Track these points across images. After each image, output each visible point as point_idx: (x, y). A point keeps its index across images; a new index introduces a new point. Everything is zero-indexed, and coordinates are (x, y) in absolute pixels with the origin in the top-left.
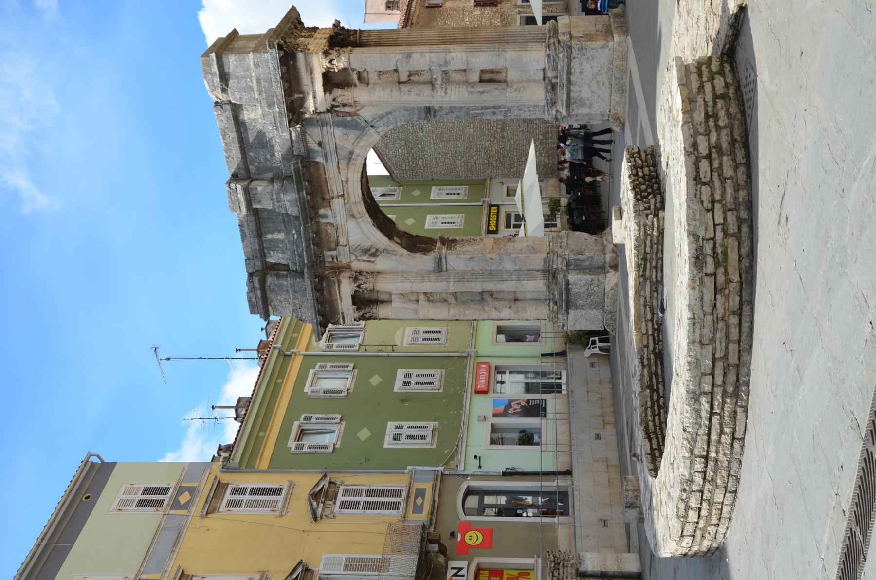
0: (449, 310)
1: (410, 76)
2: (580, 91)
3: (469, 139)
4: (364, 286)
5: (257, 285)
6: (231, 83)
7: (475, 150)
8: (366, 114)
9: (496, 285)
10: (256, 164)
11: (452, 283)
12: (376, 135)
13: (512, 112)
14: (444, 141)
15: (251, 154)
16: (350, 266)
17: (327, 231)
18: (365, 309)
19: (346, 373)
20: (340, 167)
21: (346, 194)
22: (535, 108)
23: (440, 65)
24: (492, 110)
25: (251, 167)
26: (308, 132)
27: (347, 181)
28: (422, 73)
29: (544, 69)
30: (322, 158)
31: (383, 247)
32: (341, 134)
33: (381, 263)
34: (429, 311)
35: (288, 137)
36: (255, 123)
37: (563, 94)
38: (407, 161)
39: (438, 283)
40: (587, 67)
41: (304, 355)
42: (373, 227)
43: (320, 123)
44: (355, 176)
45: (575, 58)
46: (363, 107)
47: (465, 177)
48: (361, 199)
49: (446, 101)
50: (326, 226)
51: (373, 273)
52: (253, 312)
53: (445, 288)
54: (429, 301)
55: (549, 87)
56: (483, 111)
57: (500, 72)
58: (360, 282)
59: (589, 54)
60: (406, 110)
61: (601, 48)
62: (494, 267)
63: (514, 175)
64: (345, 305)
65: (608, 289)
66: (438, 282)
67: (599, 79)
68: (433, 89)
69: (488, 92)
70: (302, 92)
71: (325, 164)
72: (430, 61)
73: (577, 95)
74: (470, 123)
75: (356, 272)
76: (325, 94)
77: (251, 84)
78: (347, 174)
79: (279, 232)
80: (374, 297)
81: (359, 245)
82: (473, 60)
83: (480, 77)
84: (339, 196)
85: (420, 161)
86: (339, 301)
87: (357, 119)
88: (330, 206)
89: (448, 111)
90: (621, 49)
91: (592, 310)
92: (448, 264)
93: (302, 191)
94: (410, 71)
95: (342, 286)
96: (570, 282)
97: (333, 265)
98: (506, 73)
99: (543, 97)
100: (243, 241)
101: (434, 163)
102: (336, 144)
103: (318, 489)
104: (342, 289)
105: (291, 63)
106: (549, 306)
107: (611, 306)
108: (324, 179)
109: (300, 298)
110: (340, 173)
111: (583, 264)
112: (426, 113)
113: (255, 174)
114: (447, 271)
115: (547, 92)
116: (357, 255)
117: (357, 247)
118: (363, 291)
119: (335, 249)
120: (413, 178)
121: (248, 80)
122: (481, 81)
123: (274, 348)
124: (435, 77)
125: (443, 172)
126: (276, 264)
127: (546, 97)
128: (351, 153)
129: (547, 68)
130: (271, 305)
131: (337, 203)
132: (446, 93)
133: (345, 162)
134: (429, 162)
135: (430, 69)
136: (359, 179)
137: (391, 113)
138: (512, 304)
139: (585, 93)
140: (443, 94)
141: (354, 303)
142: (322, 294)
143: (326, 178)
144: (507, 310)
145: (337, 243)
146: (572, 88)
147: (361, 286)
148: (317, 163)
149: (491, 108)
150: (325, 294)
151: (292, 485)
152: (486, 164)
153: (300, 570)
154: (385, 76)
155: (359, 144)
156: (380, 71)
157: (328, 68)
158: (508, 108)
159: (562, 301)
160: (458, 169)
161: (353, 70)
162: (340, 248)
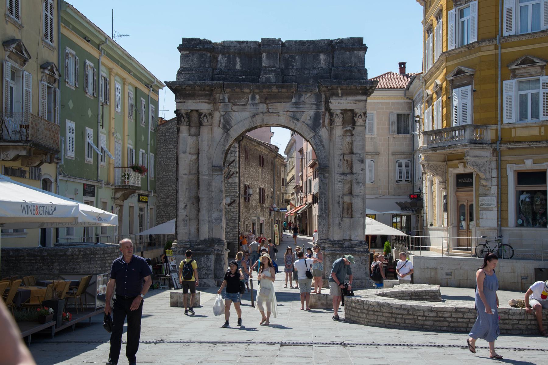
0: (186, 174)
1: (347, 161)
6: (348, 53)
8: (324, 132)
9: (206, 206)
10: (290, 59)
11: (207, 178)
15: (297, 57)
17: (243, 98)
18: (187, 118)
19: (92, 91)
20: (288, 112)
23: (356, 179)
25: (288, 55)
26: (312, 95)
29: (350, 240)
31: (230, 134)
32: (310, 115)
33: (218, 132)
34: (185, 161)
36: (318, 63)
38: (172, 137)
41: (99, 60)
43: (319, 103)
45: (360, 258)
46: (330, 131)
47: (158, 178)
52: (184, 40)
53: (204, 172)
55: (341, 242)
58: (208, 117)
61: (366, 273)
62: (214, 206)
63: (158, 213)
64: (191, 105)
69: (339, 207)
70: (342, 95)
71: (291, 103)
77: (347, 66)
79: (241, 67)
80: (192, 124)
81: (232, 118)
82: (359, 199)
85: (173, 147)
86: (194, 101)
88: (261, 103)
93: (276, 87)
94: (352, 161)
95: (206, 104)
97: (217, 99)
100: (236, 41)
101: (171, 156)
103: (55, 71)
104: (204, 104)
105: (361, 92)
106: (188, 242)
110: (285, 111)
113: (284, 57)
114: (213, 174)
116: (224, 117)
117: (230, 117)
119: (229, 102)
120: (158, 140)
121: (350, 64)
122: (343, 202)
123: (106, 39)
124: (348, 175)
125: (162, 162)
126: (217, 61)
127: (336, 241)
128: (298, 120)
129: (352, 242)
130: (188, 54)
131: (262, 107)
132: (339, 182)
134: (171, 152)
137: (323, 147)
140: (339, 180)
141: (192, 111)
143: (281, 102)
144: (185, 213)
145: (234, 104)
150: (200, 92)
151: (54, 48)
153: (26, 56)
156: (352, 143)
157: (356, 114)
160: (165, 173)
161: (354, 128)
162: (231, 105)
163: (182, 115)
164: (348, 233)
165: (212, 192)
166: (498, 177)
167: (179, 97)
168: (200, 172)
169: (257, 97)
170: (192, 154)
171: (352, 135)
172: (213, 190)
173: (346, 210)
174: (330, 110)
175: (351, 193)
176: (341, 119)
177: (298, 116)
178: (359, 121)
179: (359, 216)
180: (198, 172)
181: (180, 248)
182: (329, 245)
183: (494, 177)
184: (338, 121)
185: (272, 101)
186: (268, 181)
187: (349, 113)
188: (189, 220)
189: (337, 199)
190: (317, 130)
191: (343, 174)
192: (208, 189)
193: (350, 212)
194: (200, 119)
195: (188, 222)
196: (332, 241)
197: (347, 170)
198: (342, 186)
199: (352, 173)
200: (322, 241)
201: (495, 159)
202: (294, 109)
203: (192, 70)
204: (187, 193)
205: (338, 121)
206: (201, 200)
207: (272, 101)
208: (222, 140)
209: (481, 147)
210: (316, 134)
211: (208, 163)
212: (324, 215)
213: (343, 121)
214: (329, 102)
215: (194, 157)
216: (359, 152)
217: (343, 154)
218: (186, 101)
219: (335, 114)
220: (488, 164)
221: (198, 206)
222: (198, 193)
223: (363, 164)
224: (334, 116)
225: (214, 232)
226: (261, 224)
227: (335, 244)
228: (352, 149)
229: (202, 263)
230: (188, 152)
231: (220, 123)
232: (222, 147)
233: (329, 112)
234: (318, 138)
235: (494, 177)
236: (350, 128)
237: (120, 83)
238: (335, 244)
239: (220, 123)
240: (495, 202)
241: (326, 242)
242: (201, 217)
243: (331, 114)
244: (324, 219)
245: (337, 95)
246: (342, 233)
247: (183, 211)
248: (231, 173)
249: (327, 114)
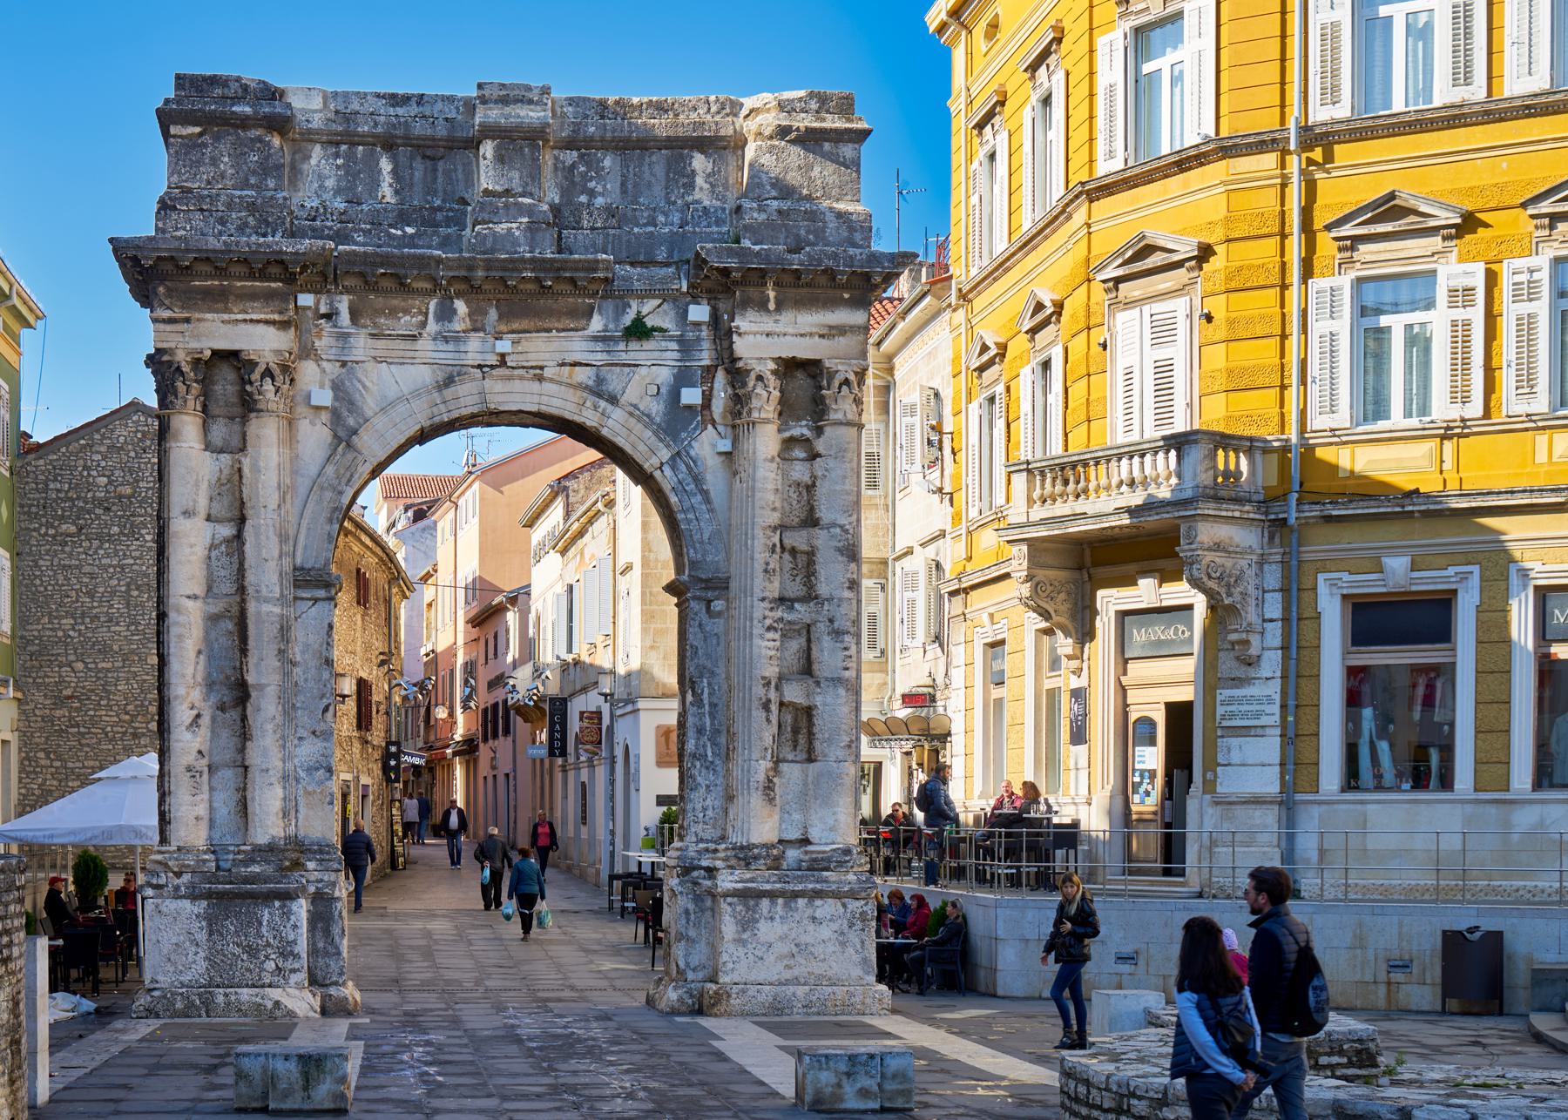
0: (195, 597)
2: (772, 919)
3: (132, 652)
4: (268, 386)
7: (100, 666)
12: (655, 461)
13: (704, 771)
16: (307, 357)
17: (406, 311)
21: (507, 372)
23: (831, 621)
27: (540, 379)
28: (798, 579)
29: (805, 841)
30: (600, 328)
35: (659, 259)
37: (768, 882)
39: (275, 578)
40: (826, 932)
42: (418, 427)
44: (556, 402)
45: (844, 906)
48: (492, 406)
49: (751, 627)
50: (420, 312)
53: (264, 591)
54: (210, 550)
55: (775, 852)
56: (707, 707)
59: (853, 937)
65: (275, 994)
66: (281, 574)
67: (798, 958)
68: (774, 601)
69: (768, 720)
72: (840, 600)
73: (765, 911)
76: (773, 359)
78: (559, 383)
80: (214, 409)
81: (364, 387)
83: (791, 703)
89: (708, 629)
90: (868, 1001)
91: (206, 958)
92: (311, 603)
94: (811, 554)
96: (288, 903)
98: (792, 761)
99: (755, 840)
102: (637, 366)
107: (228, 1004)
108: (545, 326)
110: (563, 364)
111: (319, 934)
112: (707, 581)
114: (296, 598)
115: (768, 846)
118: (251, 383)
122: (782, 704)
124: (797, 605)
127: (757, 847)
128: (613, 400)
129: (810, 848)
132: (769, 629)
133: (591, 383)
135: (816, 597)
136: (544, 409)
137: (707, 500)
138: (205, 762)
139: (767, 930)
140: (768, 622)
143: (548, 330)
146: (780, 901)
147: (269, 380)
148: (590, 316)
149: (712, 724)
152: (61, 691)
154: (795, 496)
155: (633, 421)
156: (810, 488)
158: (712, 763)
159: (231, 883)
161: (819, 431)
163: (178, 369)
164: (796, 816)
165: (294, 664)
166: (1286, 620)
168: (250, 590)
169: (461, 306)
170: (218, 521)
171: (814, 456)
172: (298, 658)
174: (734, 360)
175: (807, 669)
176: (776, 394)
177: (614, 385)
178: (842, 408)
179: (841, 754)
180: (242, 590)
181: (178, 875)
182: (733, 862)
183: (1271, 620)
184: (765, 403)
185: (515, 326)
187: (800, 375)
188: (210, 767)
189: (759, 690)
190: (684, 435)
191: (782, 600)
192: (280, 652)
193: (802, 740)
194: (248, 388)
195: (206, 776)
196: (742, 848)
197: (795, 589)
198: (778, 643)
199: (810, 597)
200: (702, 846)
201: (1276, 553)
202: (599, 356)
204: (201, 667)
205: (765, 403)
206: (253, 694)
207: (515, 326)
208: (330, 470)
209: (1237, 514)
210: (678, 453)
211: (281, 556)
212: (709, 754)
213: (781, 401)
214: (730, 333)
215: (227, 531)
216: (843, 521)
217: (782, 528)
219: (753, 375)
220: (1251, 573)
221: (244, 718)
222: (241, 670)
223: (853, 566)
225: (301, 817)
227: (756, 858)
228: (812, 509)
229: (264, 930)
230: (203, 514)
232: (328, 495)
233: (728, 371)
234: (688, 466)
235: (1271, 620)
236: (806, 432)
238: (756, 858)
240: (1276, 709)
241: (716, 851)
242: (254, 756)
244: (710, 767)
246: (776, 817)
247: (188, 736)
249: (721, 377)
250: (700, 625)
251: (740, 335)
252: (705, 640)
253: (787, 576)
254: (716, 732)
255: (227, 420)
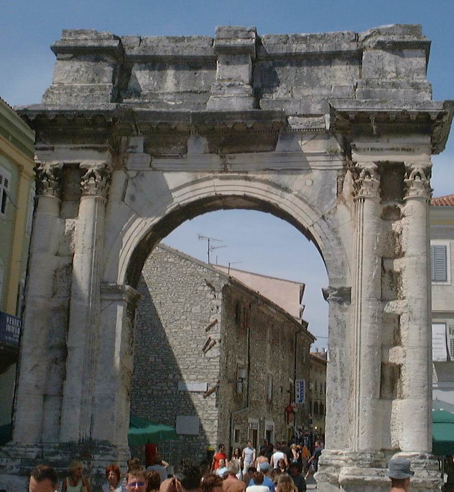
5: (106, 43)
12: (311, 223)
14: (143, 326)
18: (54, 180)
22: (340, 437)
24: (339, 378)
27: (247, 179)
35: (313, 111)
37: (370, 475)
44: (256, 191)
48: (218, 193)
51: (107, 197)
56: (338, 365)
57: (392, 392)
60: (343, 265)
70: (379, 135)
71: (273, 152)
74: (162, 359)
75: (111, 174)
76: (375, 163)
79: (175, 85)
84: (225, 164)
86: (72, 146)
87: (332, 201)
88: (211, 153)
92: (111, 302)
93: (242, 119)
108: (251, 149)
109: (82, 95)
114: (101, 300)
116: (134, 180)
119: (145, 151)
128: (286, 190)
136: (247, 194)
137: (340, 243)
141: (66, 166)
142: (88, 125)
150: (86, 129)
162: (147, 158)
167: (43, 140)
173: (388, 382)
186: (283, 366)
196: (355, 453)
203: (71, 88)
207: (234, 150)
213: (380, 187)
218: (56, 146)
224: (362, 174)
226: (269, 433)
231: (124, 194)
237: (7, 169)
239: (124, 194)
241: (341, 454)
243: (356, 171)
245: (370, 135)
248: (212, 342)
249: (348, 174)
250: (335, 316)
251: (357, 150)
252: (338, 325)
253: (387, 287)
254: (343, 380)
255: (73, 202)
